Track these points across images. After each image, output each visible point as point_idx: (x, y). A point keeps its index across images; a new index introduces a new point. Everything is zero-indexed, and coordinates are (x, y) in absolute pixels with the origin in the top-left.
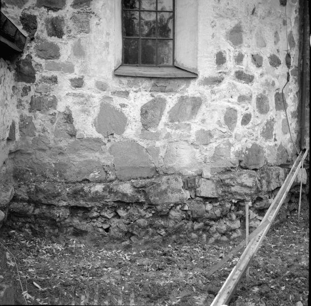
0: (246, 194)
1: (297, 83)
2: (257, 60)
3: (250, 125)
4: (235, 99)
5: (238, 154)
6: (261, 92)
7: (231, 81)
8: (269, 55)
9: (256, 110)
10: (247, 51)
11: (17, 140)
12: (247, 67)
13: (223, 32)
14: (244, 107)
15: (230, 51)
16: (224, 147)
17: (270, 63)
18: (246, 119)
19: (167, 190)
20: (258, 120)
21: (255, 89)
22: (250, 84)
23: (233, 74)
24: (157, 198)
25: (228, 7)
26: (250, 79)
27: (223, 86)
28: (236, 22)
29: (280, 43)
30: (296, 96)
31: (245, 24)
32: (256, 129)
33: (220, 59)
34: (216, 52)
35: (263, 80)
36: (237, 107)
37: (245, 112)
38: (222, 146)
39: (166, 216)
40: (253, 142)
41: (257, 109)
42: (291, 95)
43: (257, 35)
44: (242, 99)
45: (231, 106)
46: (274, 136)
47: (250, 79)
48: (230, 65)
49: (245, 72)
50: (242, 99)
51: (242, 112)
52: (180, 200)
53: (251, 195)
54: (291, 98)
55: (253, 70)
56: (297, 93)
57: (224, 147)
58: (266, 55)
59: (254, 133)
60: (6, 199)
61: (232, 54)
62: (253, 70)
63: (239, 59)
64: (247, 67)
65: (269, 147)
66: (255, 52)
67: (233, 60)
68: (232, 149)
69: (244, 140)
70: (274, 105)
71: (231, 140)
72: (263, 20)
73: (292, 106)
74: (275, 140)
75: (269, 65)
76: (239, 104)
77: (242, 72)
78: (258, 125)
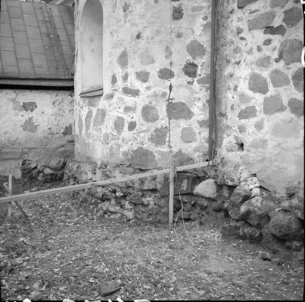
0: (118, 186)
1: (209, 91)
2: (143, 77)
3: (135, 131)
4: (122, 110)
5: (126, 154)
6: (147, 103)
7: (120, 96)
8: (158, 70)
9: (141, 119)
10: (131, 71)
12: (131, 83)
13: (115, 58)
14: (129, 116)
15: (119, 72)
16: (115, 147)
17: (159, 77)
18: (132, 126)
20: (146, 130)
21: (140, 102)
22: (137, 97)
23: (121, 90)
25: (118, 39)
26: (136, 93)
27: (115, 100)
28: (123, 49)
29: (173, 56)
30: (206, 104)
31: (129, 49)
32: (142, 135)
33: (114, 80)
34: (111, 75)
35: (151, 92)
36: (125, 116)
37: (129, 120)
38: (114, 146)
40: (139, 145)
41: (142, 118)
42: (200, 104)
43: (141, 55)
44: (127, 109)
45: (120, 115)
46: (167, 143)
47: (136, 93)
48: (120, 84)
49: (130, 87)
50: (127, 109)
51: (128, 120)
53: (121, 188)
54: (198, 107)
55: (138, 85)
56: (207, 101)
57: (115, 147)
58: (153, 71)
59: (139, 139)
61: (120, 75)
62: (138, 85)
63: (125, 78)
64: (131, 83)
65: (161, 153)
66: (139, 70)
67: (121, 79)
68: (121, 149)
69: (130, 143)
70: (165, 113)
71: (120, 142)
72: (152, 41)
73: (201, 114)
74: (170, 147)
75: (158, 78)
76: (125, 114)
77: (127, 88)
78: (144, 131)
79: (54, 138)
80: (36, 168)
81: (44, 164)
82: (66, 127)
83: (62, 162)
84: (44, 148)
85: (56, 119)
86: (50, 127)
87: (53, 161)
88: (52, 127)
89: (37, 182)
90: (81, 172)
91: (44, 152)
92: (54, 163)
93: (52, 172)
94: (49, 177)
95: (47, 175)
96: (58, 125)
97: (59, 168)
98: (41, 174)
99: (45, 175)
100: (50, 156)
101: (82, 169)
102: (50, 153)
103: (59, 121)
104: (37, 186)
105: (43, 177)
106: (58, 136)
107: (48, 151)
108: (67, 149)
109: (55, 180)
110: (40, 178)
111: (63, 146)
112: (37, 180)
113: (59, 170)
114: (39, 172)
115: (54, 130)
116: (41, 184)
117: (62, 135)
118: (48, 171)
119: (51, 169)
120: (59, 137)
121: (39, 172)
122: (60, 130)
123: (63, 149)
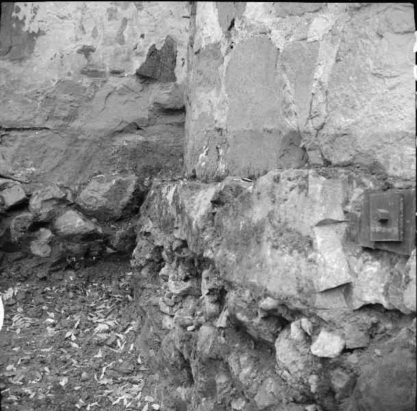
11: (178, 82)
19: (262, 231)
24: (232, 257)
39: (263, 349)
52: (300, 291)
60: (95, 195)
79: (102, 93)
80: (23, 205)
81: (59, 194)
82: (153, 52)
83: (131, 189)
84: (61, 129)
85: (112, 15)
86: (89, 44)
87: (94, 184)
88: (98, 46)
89: (27, 265)
90: (252, 235)
91: (60, 143)
92: (97, 192)
93: (90, 226)
94: (76, 247)
95: (69, 238)
96: (122, 41)
97: (117, 212)
98: (46, 234)
99: (59, 238)
100: (87, 160)
101: (258, 213)
102: (83, 149)
103: (125, 21)
104: (26, 279)
105: (51, 243)
106: (116, 83)
107: (75, 141)
108: (154, 139)
109: (102, 256)
110: (39, 248)
111: (136, 127)
112: (29, 255)
113: (119, 220)
114: (37, 225)
115: (104, 57)
116: (40, 275)
117: (135, 83)
118: (73, 222)
119: (87, 215)
120: (126, 89)
121: (37, 225)
122: (128, 60)
123: (136, 138)
